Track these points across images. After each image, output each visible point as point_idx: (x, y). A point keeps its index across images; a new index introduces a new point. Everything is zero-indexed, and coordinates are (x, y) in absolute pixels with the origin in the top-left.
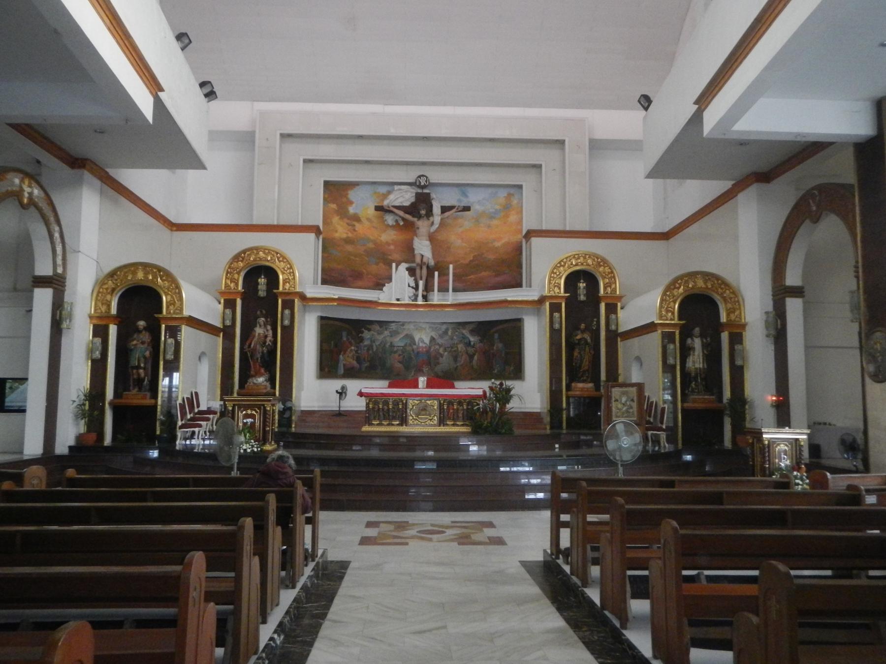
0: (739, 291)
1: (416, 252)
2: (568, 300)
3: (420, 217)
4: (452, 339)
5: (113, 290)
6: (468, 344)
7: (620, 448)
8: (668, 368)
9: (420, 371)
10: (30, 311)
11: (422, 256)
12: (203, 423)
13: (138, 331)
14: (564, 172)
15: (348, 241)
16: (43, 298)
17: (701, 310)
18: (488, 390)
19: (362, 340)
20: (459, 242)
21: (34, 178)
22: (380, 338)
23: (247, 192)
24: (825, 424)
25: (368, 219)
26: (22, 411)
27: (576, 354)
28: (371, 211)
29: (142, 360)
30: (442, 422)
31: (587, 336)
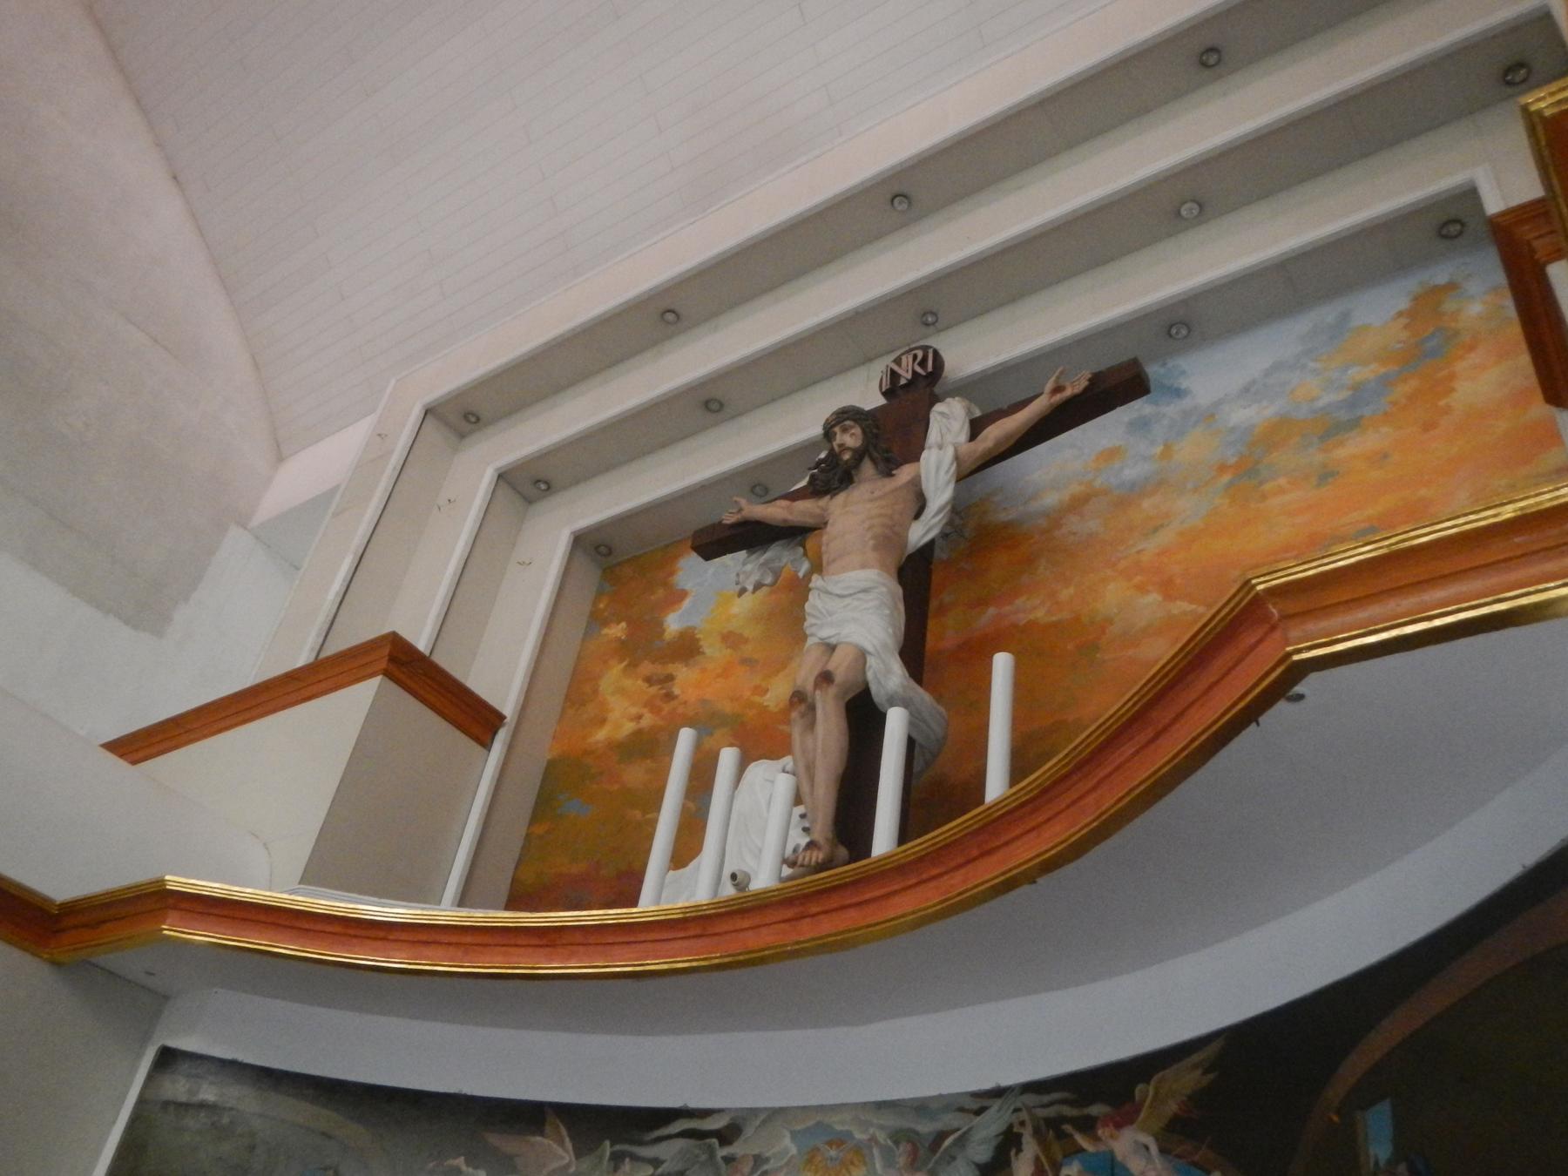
20: (1150, 605)
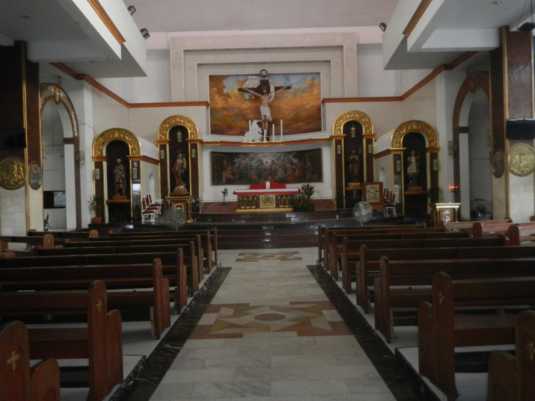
0: (436, 129)
1: (262, 114)
2: (345, 138)
3: (263, 94)
4: (283, 161)
5: (103, 143)
6: (292, 164)
7: (361, 215)
8: (396, 173)
9: (267, 179)
10: (63, 156)
11: (265, 116)
12: (155, 211)
13: (118, 164)
14: (343, 64)
15: (224, 109)
16: (69, 149)
17: (416, 141)
18: (301, 189)
19: (234, 164)
21: (58, 86)
22: (244, 162)
23: (167, 83)
24: (481, 200)
25: (235, 96)
26: (64, 207)
27: (350, 167)
28: (236, 91)
29: (121, 179)
30: (277, 206)
31: (356, 157)
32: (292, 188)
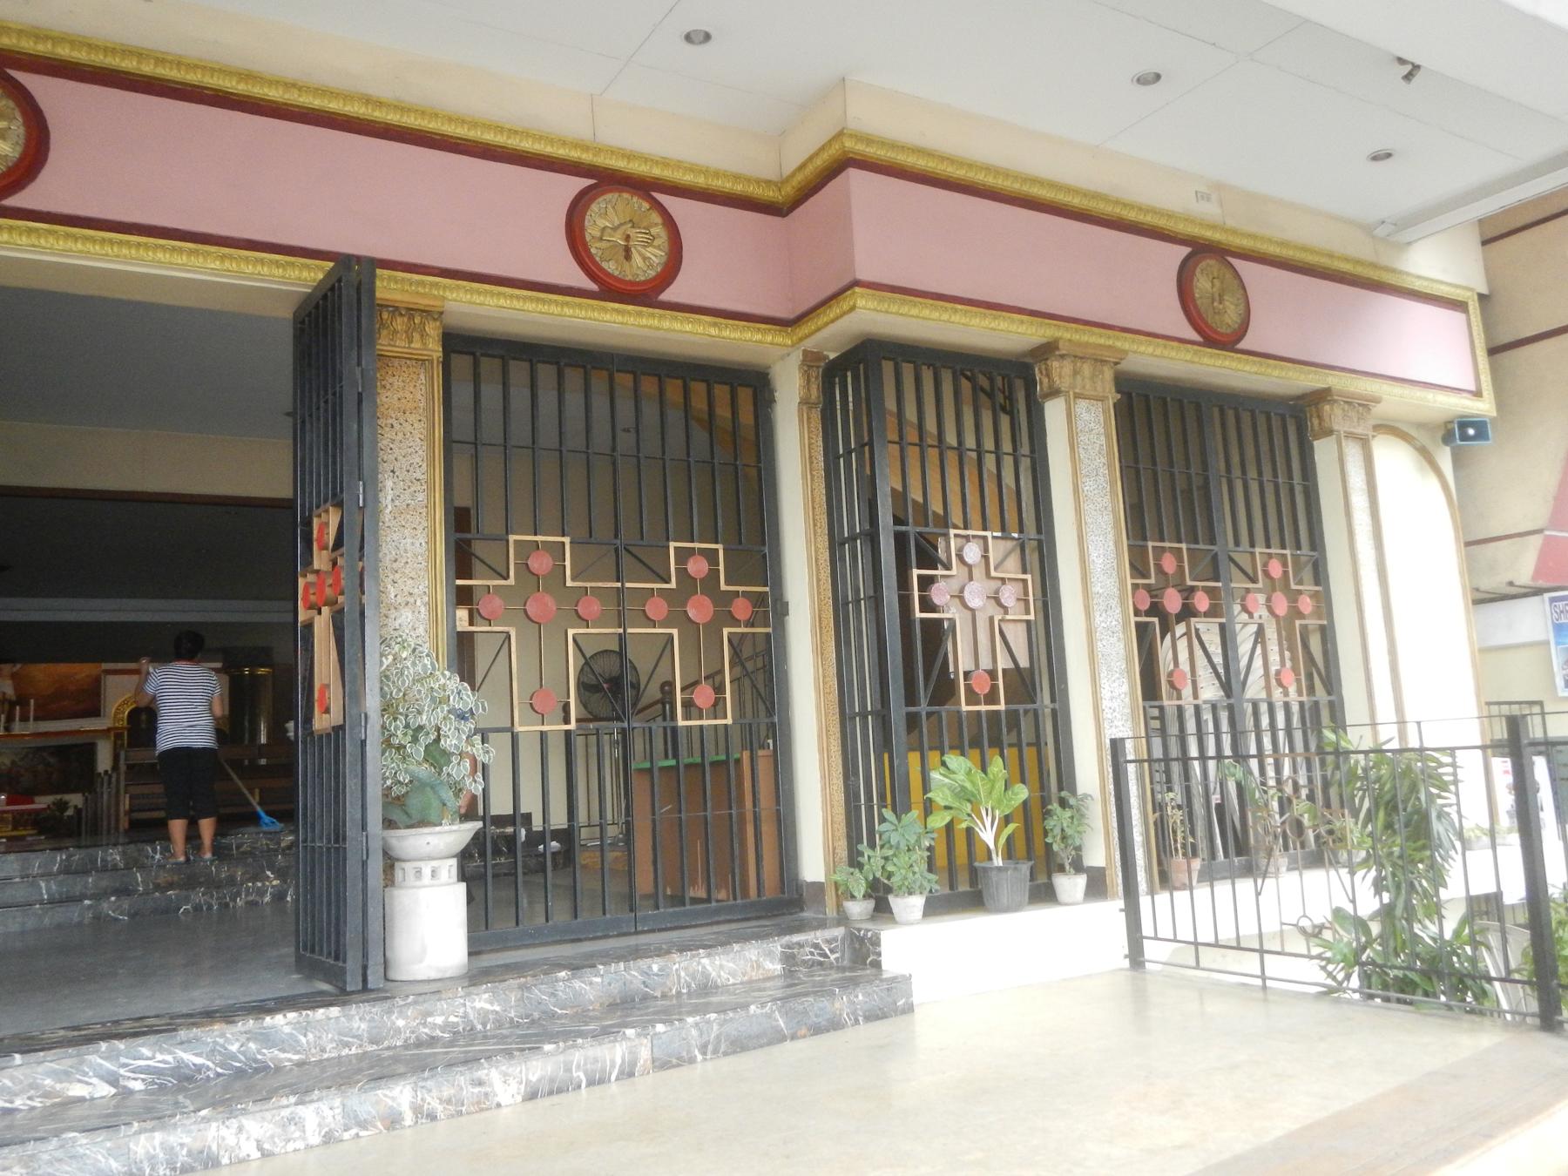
30: (15, 828)
32: (42, 802)
